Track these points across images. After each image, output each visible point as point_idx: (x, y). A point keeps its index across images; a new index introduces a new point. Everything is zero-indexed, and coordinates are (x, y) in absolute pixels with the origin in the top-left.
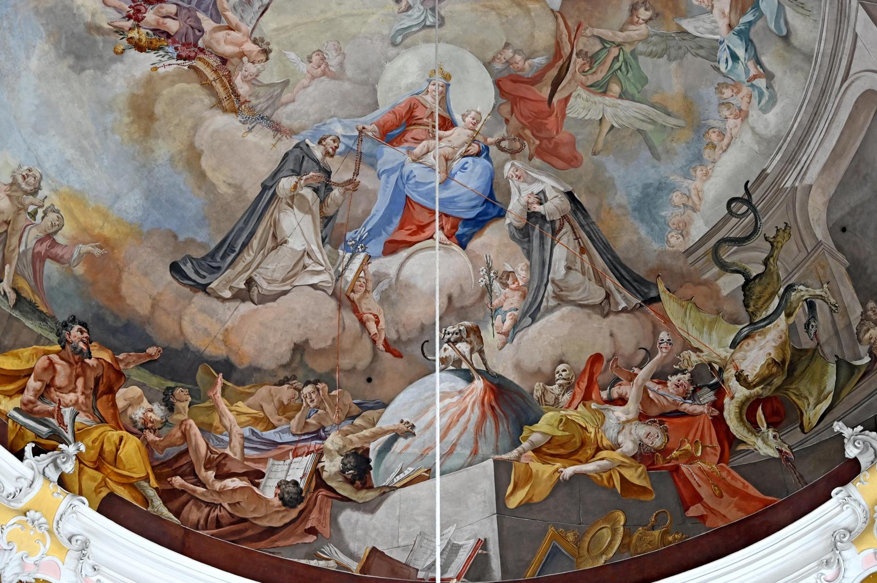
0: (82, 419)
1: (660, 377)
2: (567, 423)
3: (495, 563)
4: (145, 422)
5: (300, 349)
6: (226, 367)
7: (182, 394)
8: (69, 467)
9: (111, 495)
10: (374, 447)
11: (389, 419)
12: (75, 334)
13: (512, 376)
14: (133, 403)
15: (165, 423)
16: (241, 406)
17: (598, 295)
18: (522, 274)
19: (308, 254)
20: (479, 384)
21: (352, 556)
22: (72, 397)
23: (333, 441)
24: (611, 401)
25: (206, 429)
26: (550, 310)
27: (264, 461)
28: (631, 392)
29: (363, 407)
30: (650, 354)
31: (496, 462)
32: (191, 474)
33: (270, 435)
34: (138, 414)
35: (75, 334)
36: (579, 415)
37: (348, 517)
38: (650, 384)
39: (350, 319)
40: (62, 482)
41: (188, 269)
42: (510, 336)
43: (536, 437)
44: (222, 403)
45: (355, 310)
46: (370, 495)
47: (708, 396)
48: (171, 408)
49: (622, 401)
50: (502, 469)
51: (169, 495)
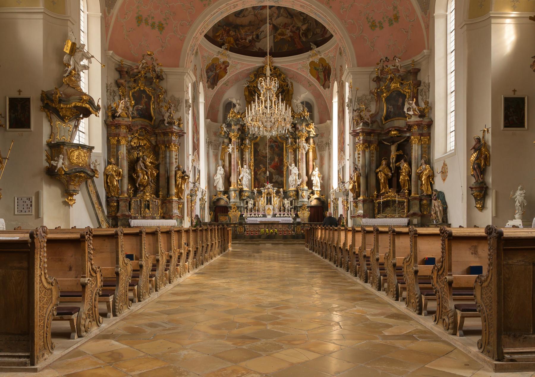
0: (226, 37)
1: (293, 27)
2: (282, 31)
3: (273, 50)
4: (233, 35)
5: (250, 22)
6: (242, 26)
7: (237, 30)
8: (226, 47)
9: (231, 47)
10: (259, 34)
11: (261, 30)
12: (225, 27)
13: (275, 24)
14: (232, 33)
15: (235, 35)
16: (244, 30)
17: (286, 16)
18: (277, 12)
19: (251, 11)
20: (272, 25)
21: (257, 49)
22: (225, 35)
23: (254, 33)
24: (287, 29)
25: (240, 34)
26: (280, 17)
27: (246, 37)
28: (290, 28)
29: (258, 28)
30: (292, 24)
31: (274, 36)
32: (239, 41)
33: (247, 33)
34: (232, 34)
35: (225, 27)
36: (283, 30)
37: (257, 44)
38: (292, 28)
39: (256, 18)
40: (226, 49)
41: (237, 15)
42: (275, 19)
43: (278, 32)
44: (242, 31)
45: (257, 16)
46: (258, 40)
47: (298, 31)
48: (236, 32)
49: (288, 29)
50: (274, 36)
51: (237, 44)
